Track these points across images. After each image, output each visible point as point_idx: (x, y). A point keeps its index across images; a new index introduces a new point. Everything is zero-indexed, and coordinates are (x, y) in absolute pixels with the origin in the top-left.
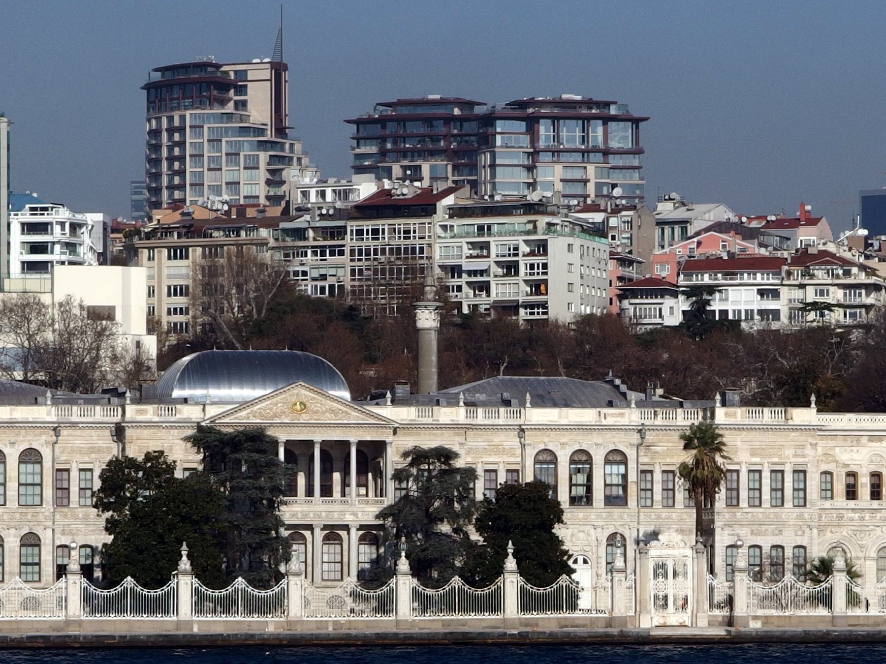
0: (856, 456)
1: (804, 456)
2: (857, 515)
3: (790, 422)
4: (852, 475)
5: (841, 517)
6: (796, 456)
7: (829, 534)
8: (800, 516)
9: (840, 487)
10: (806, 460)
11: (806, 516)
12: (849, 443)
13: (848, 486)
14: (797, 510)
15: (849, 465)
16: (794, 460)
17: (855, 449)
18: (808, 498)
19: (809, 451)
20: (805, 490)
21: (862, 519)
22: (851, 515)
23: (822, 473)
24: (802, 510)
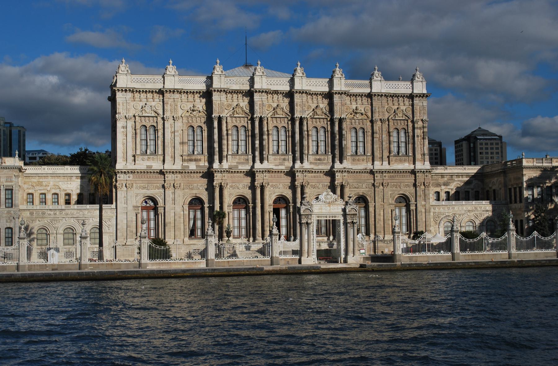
0: (69, 186)
1: (11, 181)
2: (52, 213)
3: (4, 164)
4: (69, 195)
5: (44, 213)
6: (7, 181)
7: (38, 222)
8: (9, 212)
9: (62, 200)
10: (13, 184)
11: (12, 212)
12: (66, 180)
13: (66, 200)
14: (7, 209)
15: (66, 190)
16: (5, 184)
17: (69, 182)
18: (14, 203)
19: (14, 179)
20: (12, 199)
21: (55, 214)
22: (49, 212)
23: (53, 194)
24: (10, 209)
